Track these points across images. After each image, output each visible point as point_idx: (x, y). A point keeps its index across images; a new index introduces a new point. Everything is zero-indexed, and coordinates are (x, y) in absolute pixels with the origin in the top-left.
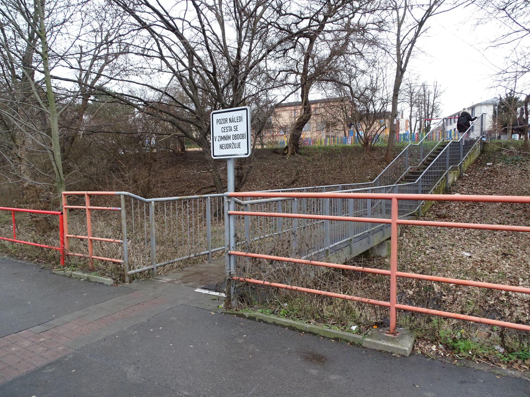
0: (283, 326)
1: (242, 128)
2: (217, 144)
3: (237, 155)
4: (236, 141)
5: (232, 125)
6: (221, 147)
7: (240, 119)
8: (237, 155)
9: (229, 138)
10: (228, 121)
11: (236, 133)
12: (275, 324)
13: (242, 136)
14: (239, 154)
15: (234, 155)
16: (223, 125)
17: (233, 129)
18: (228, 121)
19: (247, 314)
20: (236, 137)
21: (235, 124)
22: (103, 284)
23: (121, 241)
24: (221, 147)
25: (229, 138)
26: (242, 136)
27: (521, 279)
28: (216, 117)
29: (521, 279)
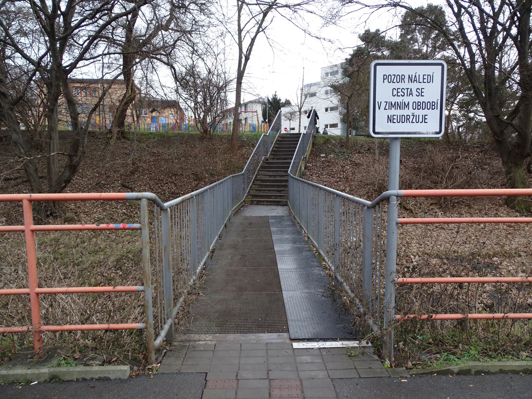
0: (515, 372)
1: (433, 92)
2: (381, 115)
3: (419, 133)
4: (420, 113)
5: (414, 86)
6: (390, 119)
7: (430, 79)
8: (419, 133)
9: (407, 106)
10: (406, 79)
11: (421, 99)
12: (502, 371)
13: (432, 106)
14: (425, 132)
15: (415, 133)
16: (396, 85)
17: (414, 93)
18: (406, 79)
19: (455, 368)
20: (418, 106)
21: (420, 86)
22: (107, 379)
23: (140, 288)
24: (390, 119)
25: (407, 106)
26: (432, 106)
27: (412, 257)
28: (381, 71)
29: (412, 257)
